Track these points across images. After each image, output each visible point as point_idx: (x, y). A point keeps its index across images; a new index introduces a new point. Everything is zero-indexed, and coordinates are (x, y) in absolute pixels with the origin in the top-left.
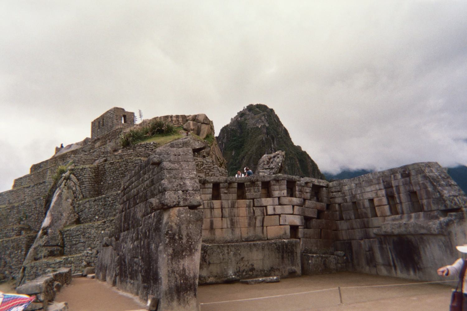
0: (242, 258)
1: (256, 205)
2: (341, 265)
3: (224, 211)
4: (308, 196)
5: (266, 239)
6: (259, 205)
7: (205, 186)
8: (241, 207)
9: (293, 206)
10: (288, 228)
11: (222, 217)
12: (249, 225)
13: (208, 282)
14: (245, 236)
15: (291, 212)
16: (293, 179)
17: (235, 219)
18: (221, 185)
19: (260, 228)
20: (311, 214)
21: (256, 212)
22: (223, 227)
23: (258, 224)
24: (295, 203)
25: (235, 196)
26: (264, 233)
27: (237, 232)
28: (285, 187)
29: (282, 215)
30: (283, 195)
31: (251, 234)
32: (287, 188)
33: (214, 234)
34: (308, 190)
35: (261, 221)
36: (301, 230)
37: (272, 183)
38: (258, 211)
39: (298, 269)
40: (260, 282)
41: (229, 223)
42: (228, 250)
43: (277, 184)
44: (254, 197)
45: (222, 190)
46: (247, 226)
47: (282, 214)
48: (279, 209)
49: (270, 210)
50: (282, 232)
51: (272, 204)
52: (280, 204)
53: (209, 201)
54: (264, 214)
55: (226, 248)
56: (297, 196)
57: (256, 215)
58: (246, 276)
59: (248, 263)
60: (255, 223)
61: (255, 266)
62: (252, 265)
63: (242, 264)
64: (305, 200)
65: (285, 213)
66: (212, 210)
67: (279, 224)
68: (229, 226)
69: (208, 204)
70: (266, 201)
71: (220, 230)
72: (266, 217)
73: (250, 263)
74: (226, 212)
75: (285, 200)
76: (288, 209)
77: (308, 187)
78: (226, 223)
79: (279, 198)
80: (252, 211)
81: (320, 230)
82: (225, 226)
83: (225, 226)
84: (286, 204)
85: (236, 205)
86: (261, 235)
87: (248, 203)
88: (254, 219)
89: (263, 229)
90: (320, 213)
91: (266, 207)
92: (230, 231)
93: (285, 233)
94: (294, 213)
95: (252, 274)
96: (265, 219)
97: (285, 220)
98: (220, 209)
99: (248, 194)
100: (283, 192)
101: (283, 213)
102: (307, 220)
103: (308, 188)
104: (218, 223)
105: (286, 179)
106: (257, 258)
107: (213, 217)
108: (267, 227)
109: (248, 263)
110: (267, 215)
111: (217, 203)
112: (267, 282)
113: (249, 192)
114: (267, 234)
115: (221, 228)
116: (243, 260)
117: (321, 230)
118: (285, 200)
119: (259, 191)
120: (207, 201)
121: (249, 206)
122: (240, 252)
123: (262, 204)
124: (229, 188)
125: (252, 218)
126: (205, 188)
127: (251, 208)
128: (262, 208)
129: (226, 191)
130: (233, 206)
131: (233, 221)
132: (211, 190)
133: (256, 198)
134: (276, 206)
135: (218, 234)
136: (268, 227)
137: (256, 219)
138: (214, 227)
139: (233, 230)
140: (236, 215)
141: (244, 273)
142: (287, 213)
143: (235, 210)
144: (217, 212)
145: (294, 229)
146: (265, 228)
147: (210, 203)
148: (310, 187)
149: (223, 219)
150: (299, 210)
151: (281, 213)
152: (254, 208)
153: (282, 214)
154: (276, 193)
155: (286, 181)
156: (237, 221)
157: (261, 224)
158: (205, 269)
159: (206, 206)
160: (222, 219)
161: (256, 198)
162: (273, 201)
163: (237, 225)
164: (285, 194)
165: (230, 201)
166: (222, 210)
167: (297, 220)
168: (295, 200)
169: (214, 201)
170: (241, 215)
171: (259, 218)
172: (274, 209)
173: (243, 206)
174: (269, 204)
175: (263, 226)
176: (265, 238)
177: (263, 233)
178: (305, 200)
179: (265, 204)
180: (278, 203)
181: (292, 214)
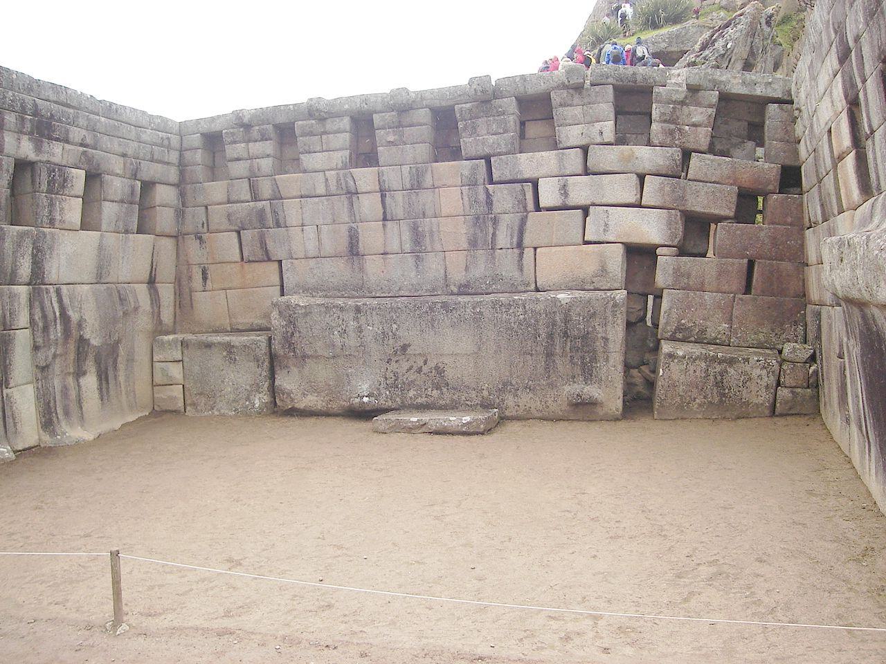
0: (404, 348)
1: (495, 177)
2: (793, 392)
3: (388, 200)
4: (702, 137)
5: (533, 287)
6: (509, 177)
7: (324, 126)
8: (444, 186)
9: (641, 178)
10: (615, 258)
11: (385, 219)
12: (473, 243)
13: (301, 405)
14: (458, 276)
15: (632, 199)
16: (639, 78)
17: (425, 224)
18: (377, 119)
19: (510, 251)
20: (701, 201)
21: (494, 199)
22: (388, 250)
23: (504, 238)
24: (646, 166)
25: (423, 150)
26: (525, 269)
27: (433, 265)
28: (606, 108)
29: (592, 209)
30: (599, 140)
31: (480, 270)
32: (617, 113)
33: (362, 269)
34: (700, 114)
35: (516, 228)
36: (666, 260)
37: (556, 98)
38: (504, 198)
39: (611, 395)
40: (410, 430)
41: (407, 236)
42: (356, 319)
43: (576, 100)
44: (487, 150)
45: (380, 133)
46: (465, 246)
47: (594, 205)
48: (581, 190)
49: (549, 195)
50: (590, 268)
51: (556, 172)
52: (587, 172)
53: (342, 172)
54: (525, 207)
55: (352, 314)
56: (656, 142)
57: (497, 208)
58: (419, 400)
59: (425, 363)
60: (494, 234)
61: (450, 374)
62: (439, 371)
63: (405, 366)
64: (686, 155)
65: (604, 201)
66: (354, 198)
67: (580, 241)
68: (408, 247)
69: (338, 181)
70: (529, 163)
71: (379, 258)
72: (533, 217)
73: (431, 364)
74: (398, 203)
75: (605, 157)
76: (622, 189)
77: (698, 104)
78: (398, 236)
79: (585, 150)
80: (482, 197)
81: (746, 261)
82: (395, 246)
83: (395, 246)
84: (608, 168)
85: (428, 181)
86: (516, 274)
87: (466, 172)
88: (490, 224)
89: (521, 255)
90: (747, 203)
91: (535, 184)
92: (410, 259)
93: (603, 271)
94: (643, 203)
95: (440, 398)
96: (529, 223)
97: (606, 225)
98: (379, 195)
99: (468, 144)
100: (598, 126)
101: (597, 202)
102: (695, 229)
103: (700, 110)
104: (371, 237)
105: (610, 80)
106: (454, 348)
107: (358, 218)
108: (535, 249)
109: (425, 363)
110: (538, 208)
111: (365, 177)
112: (437, 433)
113: (471, 136)
114: (155, 275)
115: (382, 252)
116: (409, 351)
117: (751, 264)
118: (605, 157)
119: (506, 131)
120: (333, 172)
121: (473, 184)
122: (397, 330)
123: (520, 172)
124: (400, 125)
125: (483, 219)
126: (325, 133)
127: (481, 189)
128: (518, 186)
129: (391, 138)
130: (417, 185)
131: (420, 229)
132: (347, 136)
133: (500, 154)
134: (571, 180)
135: (374, 268)
136: (538, 250)
137: (495, 221)
138: (361, 249)
139: (418, 259)
140: (429, 212)
141: (412, 393)
142: (611, 202)
143: (425, 197)
144: (369, 205)
145: (640, 255)
146: (528, 253)
147: (345, 175)
148: (710, 106)
149: (389, 224)
150: (661, 189)
151: (588, 202)
152: (490, 187)
153: (594, 205)
154: (572, 135)
155: (610, 89)
156: (431, 232)
157: (515, 240)
158: (294, 370)
159: (333, 189)
160: (384, 226)
161: (500, 154)
162: (561, 160)
163: (432, 241)
164: (609, 135)
165: (406, 169)
166: (383, 197)
167: (651, 228)
168: (646, 156)
169: (357, 172)
170: (445, 211)
171: (508, 221)
172: (564, 190)
173: (450, 183)
174: (544, 170)
175: (520, 245)
176: (528, 285)
177: (521, 269)
178: (686, 155)
179: (527, 174)
180: (579, 168)
181: (639, 205)
